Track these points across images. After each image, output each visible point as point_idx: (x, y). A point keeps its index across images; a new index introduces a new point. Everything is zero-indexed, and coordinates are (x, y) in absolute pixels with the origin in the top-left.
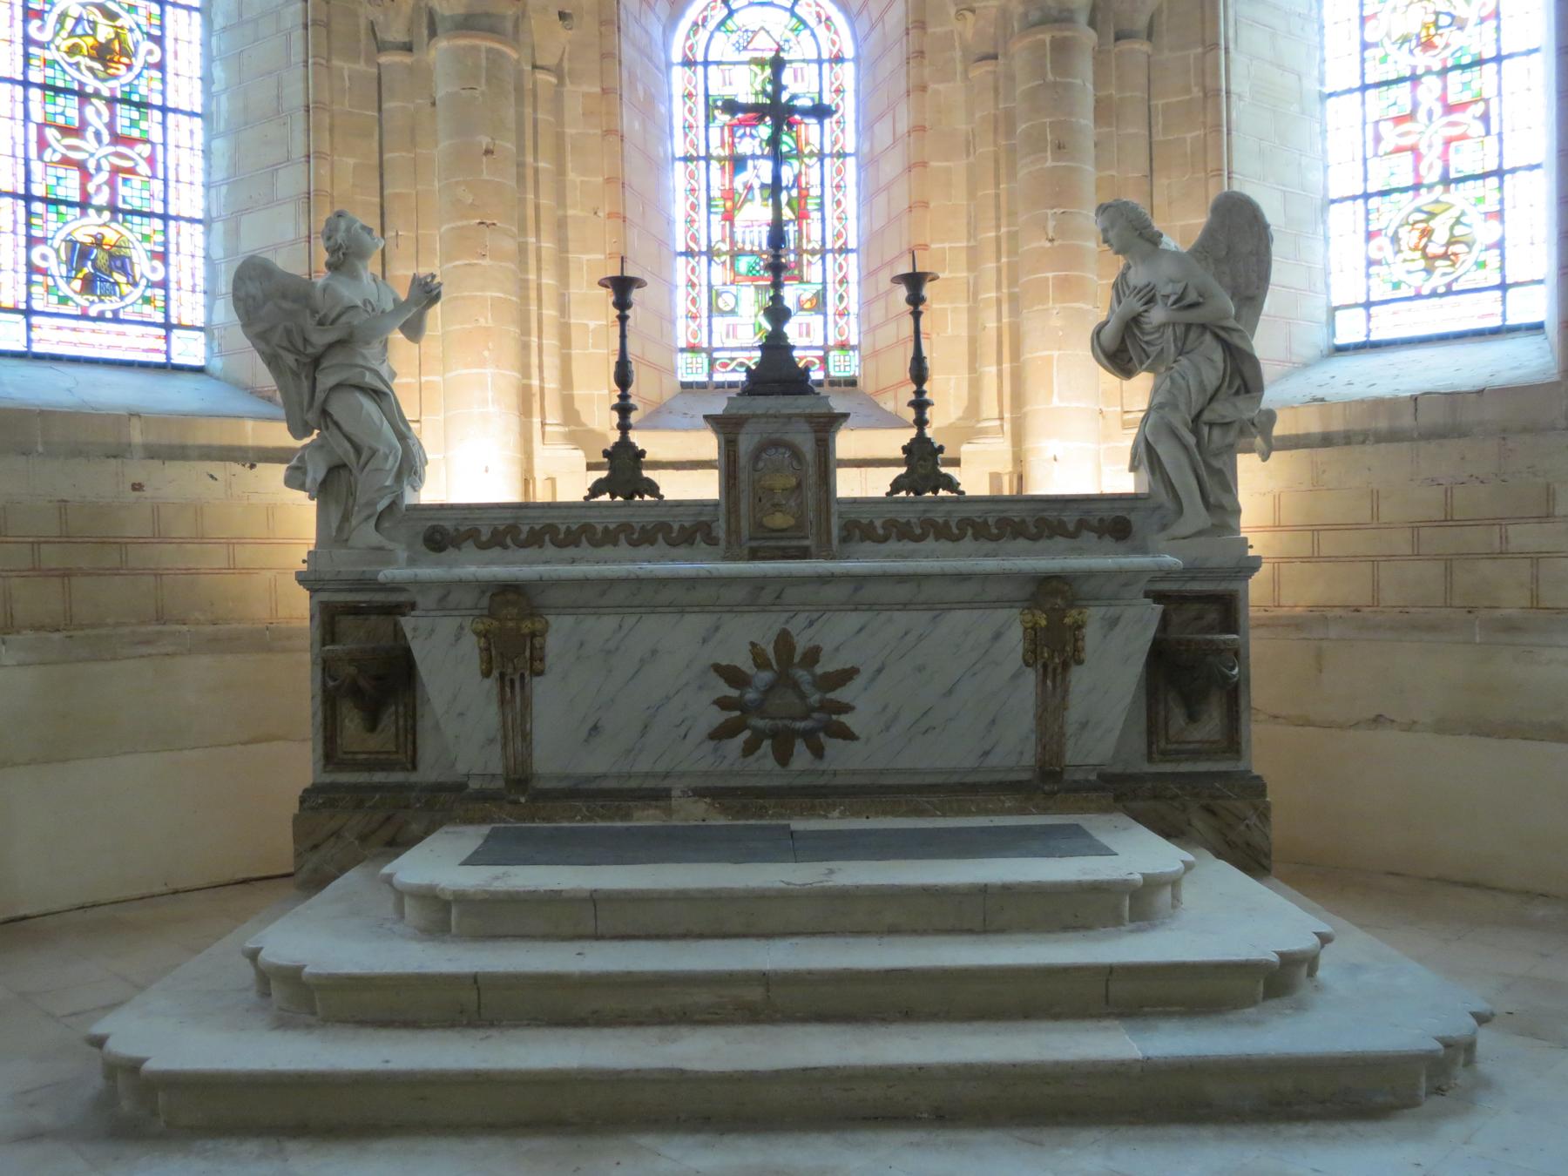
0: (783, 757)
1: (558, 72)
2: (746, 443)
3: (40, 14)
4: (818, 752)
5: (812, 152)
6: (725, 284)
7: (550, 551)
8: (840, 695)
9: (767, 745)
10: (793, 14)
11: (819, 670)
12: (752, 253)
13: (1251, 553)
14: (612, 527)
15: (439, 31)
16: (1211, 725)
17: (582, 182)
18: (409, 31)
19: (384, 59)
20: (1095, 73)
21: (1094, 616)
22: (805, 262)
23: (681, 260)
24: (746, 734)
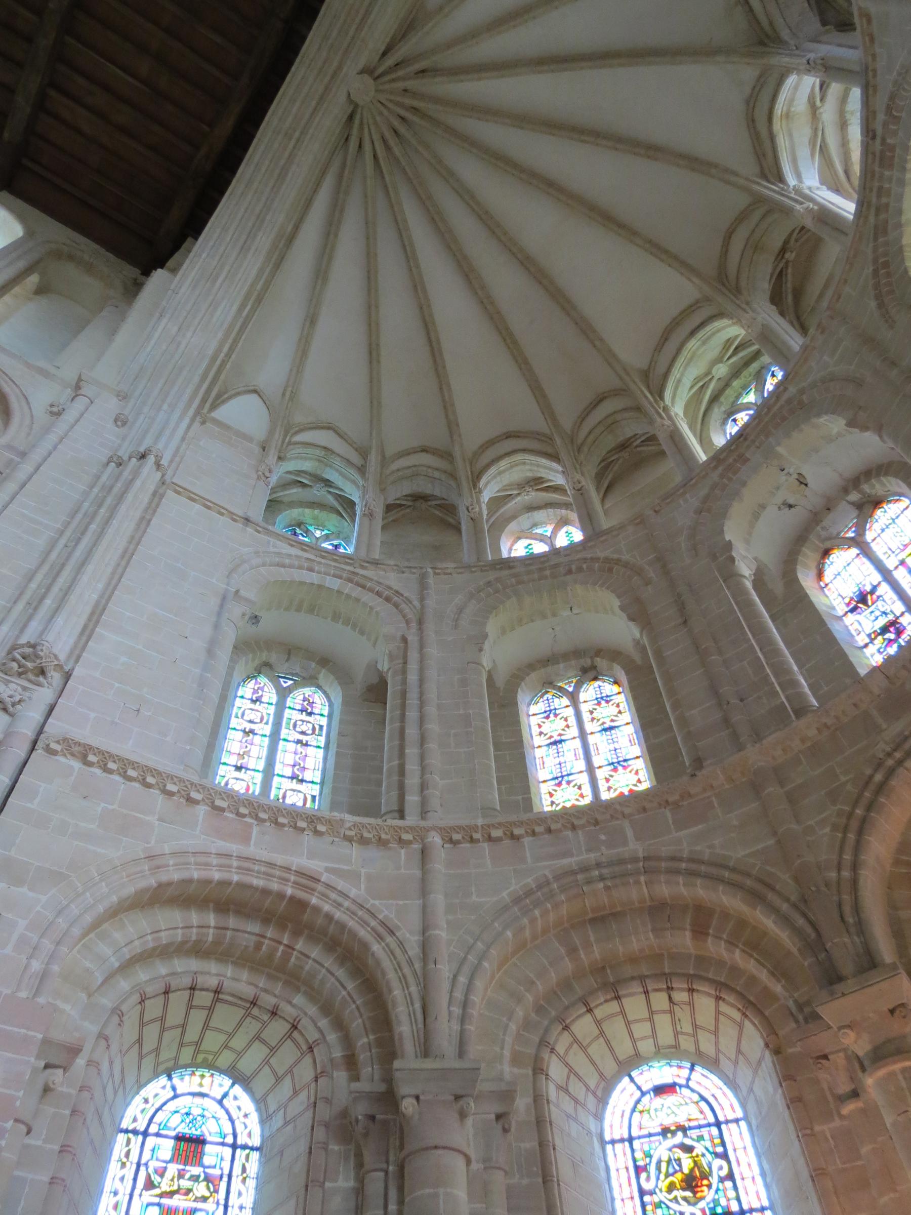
3: (645, 1169)
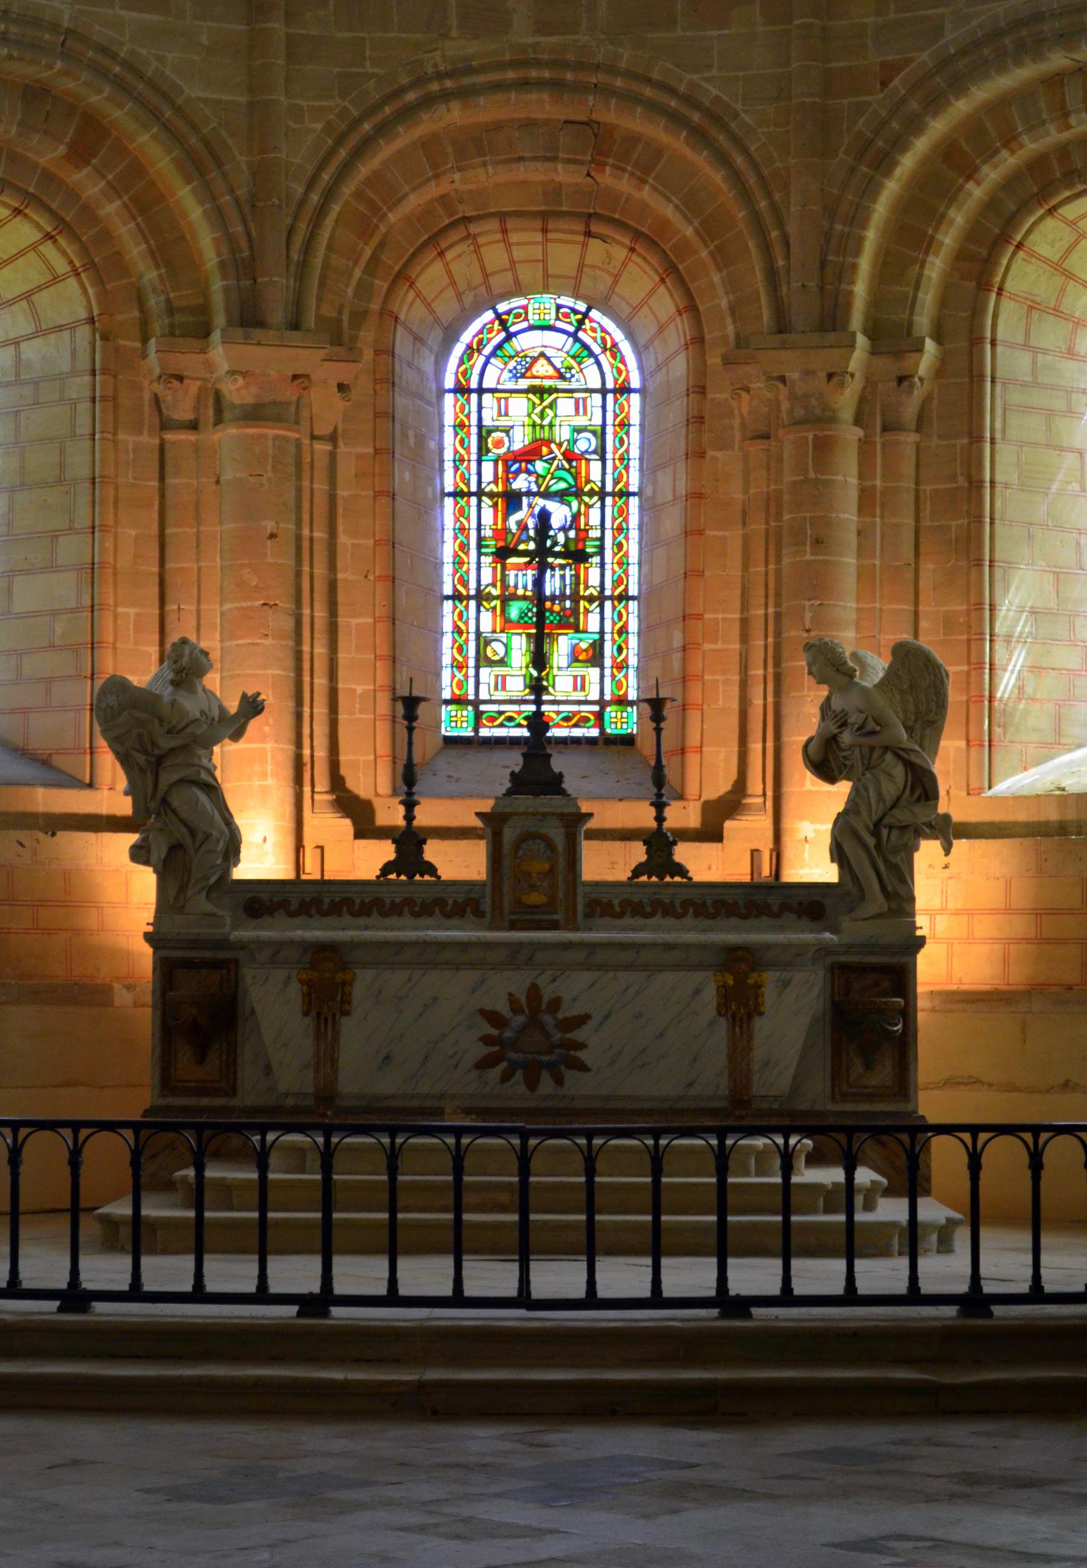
0: (532, 1084)
1: (333, 439)
2: (509, 835)
4: (559, 1081)
5: (592, 489)
6: (494, 631)
7: (347, 919)
8: (579, 1035)
9: (519, 1074)
10: (577, 339)
11: (560, 1015)
12: (524, 598)
13: (919, 933)
14: (398, 900)
15: (227, 415)
16: (883, 1075)
17: (353, 545)
18: (197, 409)
19: (169, 436)
20: (860, 464)
21: (770, 978)
22: (582, 610)
23: (448, 605)
24: (504, 1065)
